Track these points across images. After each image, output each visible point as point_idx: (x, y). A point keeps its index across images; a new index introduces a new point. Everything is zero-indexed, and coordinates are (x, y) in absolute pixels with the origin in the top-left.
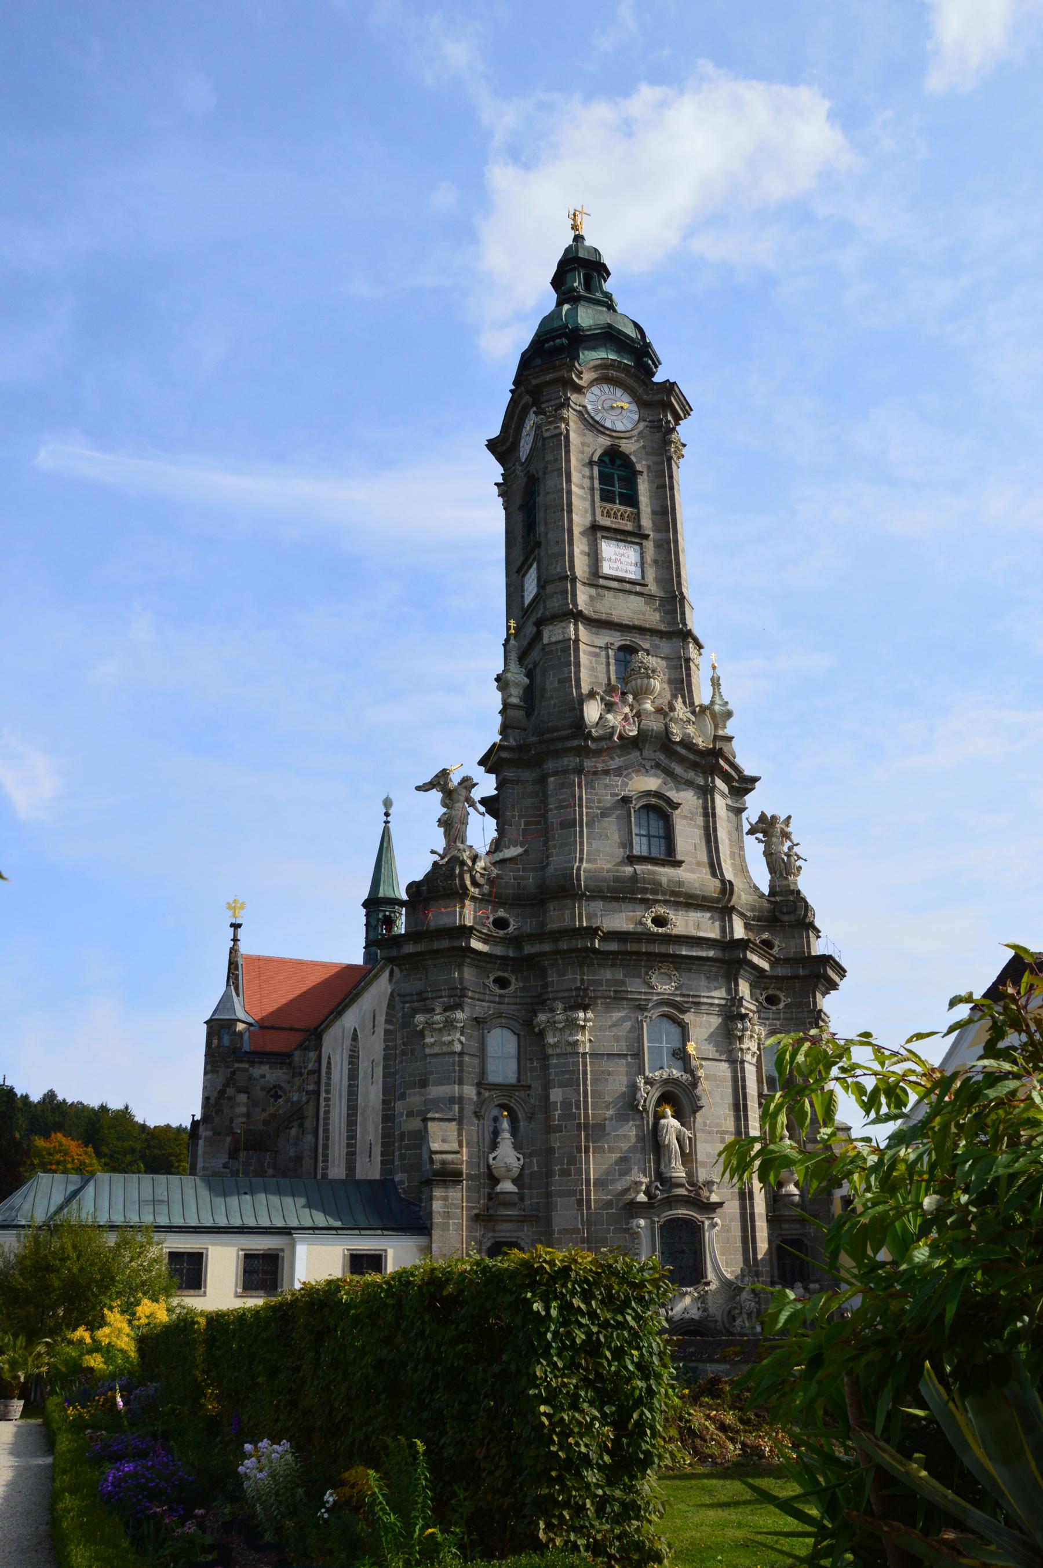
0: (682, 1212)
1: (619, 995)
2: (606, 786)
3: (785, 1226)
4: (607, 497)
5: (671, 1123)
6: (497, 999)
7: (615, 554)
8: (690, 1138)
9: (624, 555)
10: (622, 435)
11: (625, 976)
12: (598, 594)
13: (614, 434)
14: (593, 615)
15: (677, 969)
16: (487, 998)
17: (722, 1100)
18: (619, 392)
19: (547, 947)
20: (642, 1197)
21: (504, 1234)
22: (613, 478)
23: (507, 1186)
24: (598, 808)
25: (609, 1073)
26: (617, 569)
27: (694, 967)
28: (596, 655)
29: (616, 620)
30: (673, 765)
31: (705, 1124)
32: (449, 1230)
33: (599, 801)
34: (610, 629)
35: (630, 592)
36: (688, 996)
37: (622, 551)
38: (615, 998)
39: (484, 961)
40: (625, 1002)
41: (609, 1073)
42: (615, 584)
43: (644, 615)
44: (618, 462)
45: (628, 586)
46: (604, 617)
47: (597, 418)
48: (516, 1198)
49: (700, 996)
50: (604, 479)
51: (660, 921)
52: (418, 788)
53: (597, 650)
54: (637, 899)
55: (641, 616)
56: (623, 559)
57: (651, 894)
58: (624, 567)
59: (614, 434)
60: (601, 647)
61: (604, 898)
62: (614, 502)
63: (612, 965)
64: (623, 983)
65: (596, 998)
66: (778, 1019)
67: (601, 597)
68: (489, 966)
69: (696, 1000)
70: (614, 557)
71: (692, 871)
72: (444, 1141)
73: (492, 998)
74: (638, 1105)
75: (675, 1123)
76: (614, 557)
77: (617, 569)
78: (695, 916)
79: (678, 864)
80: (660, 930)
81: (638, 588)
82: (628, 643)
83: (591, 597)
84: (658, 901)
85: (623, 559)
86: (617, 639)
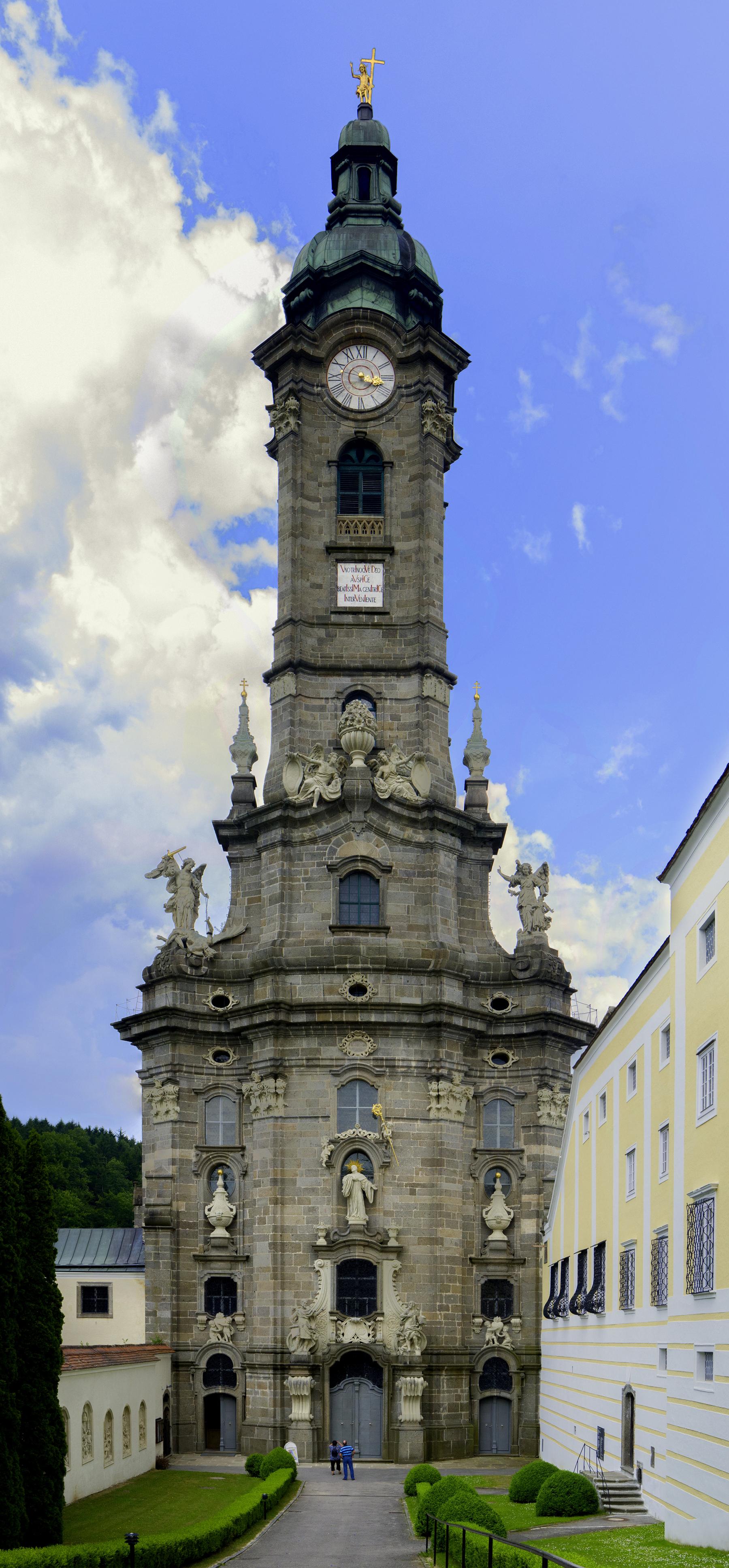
0: (358, 1254)
1: (311, 1063)
2: (313, 856)
3: (491, 1268)
4: (346, 505)
5: (355, 1178)
7: (353, 580)
8: (375, 1192)
9: (363, 579)
10: (369, 416)
11: (320, 1044)
12: (328, 635)
13: (360, 417)
14: (320, 663)
15: (371, 1035)
17: (415, 1155)
18: (371, 352)
19: (245, 1022)
20: (322, 1242)
21: (216, 1271)
22: (356, 479)
23: (220, 1232)
24: (305, 880)
26: (354, 599)
27: (390, 1033)
28: (322, 709)
29: (346, 662)
30: (386, 825)
31: (394, 1178)
32: (159, 1267)
33: (306, 872)
34: (339, 675)
35: (366, 625)
36: (382, 1060)
37: (361, 575)
38: (308, 1066)
42: (349, 619)
43: (381, 650)
44: (368, 454)
45: (364, 618)
46: (332, 662)
47: (340, 399)
48: (504, 1245)
49: (394, 1060)
50: (346, 482)
51: (359, 989)
53: (323, 702)
54: (334, 969)
55: (377, 654)
56: (362, 585)
57: (351, 963)
58: (362, 594)
59: (360, 417)
60: (327, 699)
61: (302, 971)
62: (356, 512)
63: (307, 1035)
64: (318, 1051)
67: (331, 637)
69: (391, 1063)
70: (350, 585)
71: (401, 936)
72: (159, 1196)
74: (321, 1163)
75: (362, 1177)
76: (350, 585)
77: (354, 599)
78: (397, 980)
79: (385, 930)
80: (359, 999)
81: (376, 619)
82: (359, 688)
83: (321, 641)
84: (357, 970)
85: (362, 585)
86: (345, 682)
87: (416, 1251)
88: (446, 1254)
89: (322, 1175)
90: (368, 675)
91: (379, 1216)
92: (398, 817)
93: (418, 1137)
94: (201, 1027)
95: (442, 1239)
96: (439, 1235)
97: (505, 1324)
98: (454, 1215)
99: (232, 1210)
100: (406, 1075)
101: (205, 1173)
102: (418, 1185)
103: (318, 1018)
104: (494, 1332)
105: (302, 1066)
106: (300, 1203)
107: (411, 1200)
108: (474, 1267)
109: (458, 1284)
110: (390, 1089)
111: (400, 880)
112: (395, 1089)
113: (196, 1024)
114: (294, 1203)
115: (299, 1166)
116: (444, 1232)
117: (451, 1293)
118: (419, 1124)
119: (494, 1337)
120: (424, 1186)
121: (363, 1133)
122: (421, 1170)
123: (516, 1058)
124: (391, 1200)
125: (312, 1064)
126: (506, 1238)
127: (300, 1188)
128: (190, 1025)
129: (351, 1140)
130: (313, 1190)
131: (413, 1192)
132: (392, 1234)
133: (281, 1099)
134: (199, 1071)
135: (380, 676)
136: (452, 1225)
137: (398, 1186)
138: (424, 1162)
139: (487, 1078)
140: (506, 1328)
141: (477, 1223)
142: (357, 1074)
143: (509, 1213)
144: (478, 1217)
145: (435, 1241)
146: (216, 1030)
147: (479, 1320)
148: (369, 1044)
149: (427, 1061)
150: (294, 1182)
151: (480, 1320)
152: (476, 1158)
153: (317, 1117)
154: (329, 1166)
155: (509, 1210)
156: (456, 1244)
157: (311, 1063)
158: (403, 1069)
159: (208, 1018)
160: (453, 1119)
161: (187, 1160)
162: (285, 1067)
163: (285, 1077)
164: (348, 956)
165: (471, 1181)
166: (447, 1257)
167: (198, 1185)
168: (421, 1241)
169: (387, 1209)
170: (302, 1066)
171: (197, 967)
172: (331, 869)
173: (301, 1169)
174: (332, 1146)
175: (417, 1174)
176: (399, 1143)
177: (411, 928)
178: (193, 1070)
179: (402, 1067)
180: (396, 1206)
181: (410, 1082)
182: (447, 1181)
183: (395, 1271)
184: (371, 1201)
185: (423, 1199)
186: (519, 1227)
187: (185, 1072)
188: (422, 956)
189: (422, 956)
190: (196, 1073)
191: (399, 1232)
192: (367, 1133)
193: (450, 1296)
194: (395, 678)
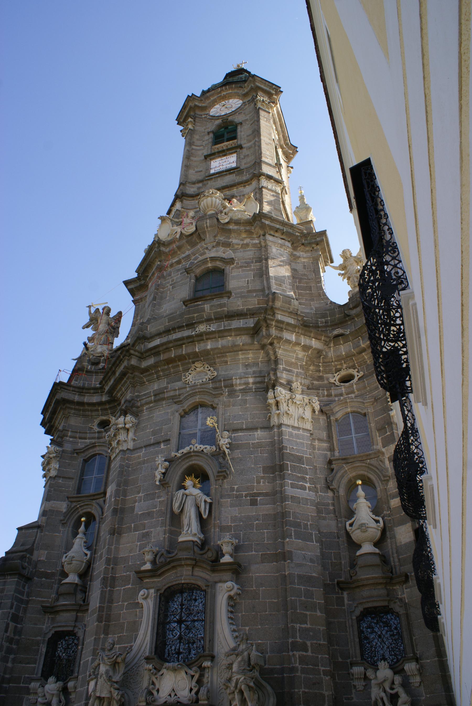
1: (158, 398)
6: (96, 435)
15: (211, 365)
16: (88, 435)
25: (144, 462)
31: (232, 489)
39: (88, 410)
40: (164, 402)
41: (144, 462)
52: (83, 328)
63: (158, 378)
65: (142, 405)
66: (353, 392)
68: (94, 413)
73: (93, 435)
75: (196, 492)
87: (259, 571)
88: (297, 572)
89: (159, 497)
90: (226, 191)
91: (214, 531)
92: (238, 232)
93: (259, 445)
94: (86, 399)
95: (290, 552)
96: (287, 548)
97: (395, 673)
98: (306, 525)
99: (86, 555)
100: (245, 391)
101: (72, 522)
102: (259, 494)
103: (162, 357)
104: (381, 685)
105: (151, 402)
106: (135, 530)
107: (251, 511)
108: (345, 595)
109: (319, 614)
110: (229, 406)
111: (241, 267)
112: (233, 406)
113: (82, 398)
114: (131, 531)
115: (139, 493)
116: (293, 543)
117: (309, 626)
118: (259, 433)
119: (383, 694)
120: (266, 494)
121: (200, 447)
122: (262, 478)
123: (361, 374)
124: (229, 513)
125: (159, 397)
126: (377, 551)
127: (137, 514)
128: (76, 398)
129: (187, 456)
130: (149, 514)
131: (254, 503)
132: (226, 549)
133: (131, 435)
134: (83, 435)
135: (233, 189)
136: (308, 538)
137: (237, 497)
138: (265, 470)
139: (336, 396)
140: (398, 679)
141: (343, 539)
142: (197, 399)
143: (377, 521)
144: (343, 532)
145: (284, 556)
146: (99, 400)
147: (357, 670)
148: (209, 373)
149: (265, 376)
150: (133, 508)
151: (362, 669)
152: (332, 470)
153: (158, 443)
154: (164, 483)
155: (377, 518)
156: (312, 561)
157: (158, 398)
158: (242, 387)
159: (92, 391)
160: (296, 425)
161: (57, 511)
162: (138, 407)
163: (136, 415)
164: (195, 315)
165: (330, 494)
166: (300, 576)
167: (62, 533)
168: (265, 559)
169: (224, 524)
170: (151, 402)
171: (97, 364)
172: (188, 271)
173: (140, 495)
174: (167, 463)
175: (258, 482)
176: (237, 454)
177: (249, 291)
178: (78, 435)
179: (240, 384)
180: (234, 519)
181: (249, 398)
182: (293, 486)
183: (230, 598)
184: (205, 517)
185: (265, 508)
186: (394, 537)
187: (71, 437)
188: (258, 304)
189: (258, 304)
190: (80, 438)
191: (237, 549)
192: (203, 447)
193: (307, 630)
194: (243, 188)
